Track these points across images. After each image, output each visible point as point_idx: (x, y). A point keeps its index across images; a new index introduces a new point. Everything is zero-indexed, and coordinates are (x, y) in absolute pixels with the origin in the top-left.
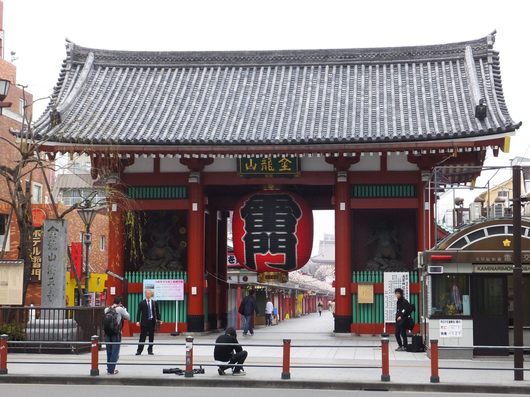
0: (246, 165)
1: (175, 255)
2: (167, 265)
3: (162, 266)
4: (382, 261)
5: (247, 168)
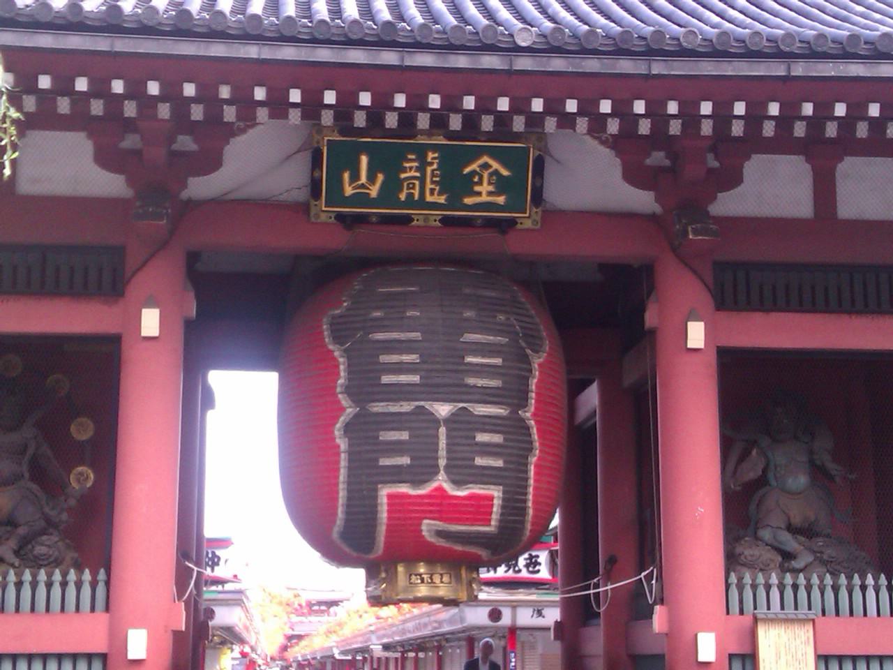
0: (346, 176)
1: (53, 513)
2: (21, 548)
4: (790, 542)
5: (349, 191)
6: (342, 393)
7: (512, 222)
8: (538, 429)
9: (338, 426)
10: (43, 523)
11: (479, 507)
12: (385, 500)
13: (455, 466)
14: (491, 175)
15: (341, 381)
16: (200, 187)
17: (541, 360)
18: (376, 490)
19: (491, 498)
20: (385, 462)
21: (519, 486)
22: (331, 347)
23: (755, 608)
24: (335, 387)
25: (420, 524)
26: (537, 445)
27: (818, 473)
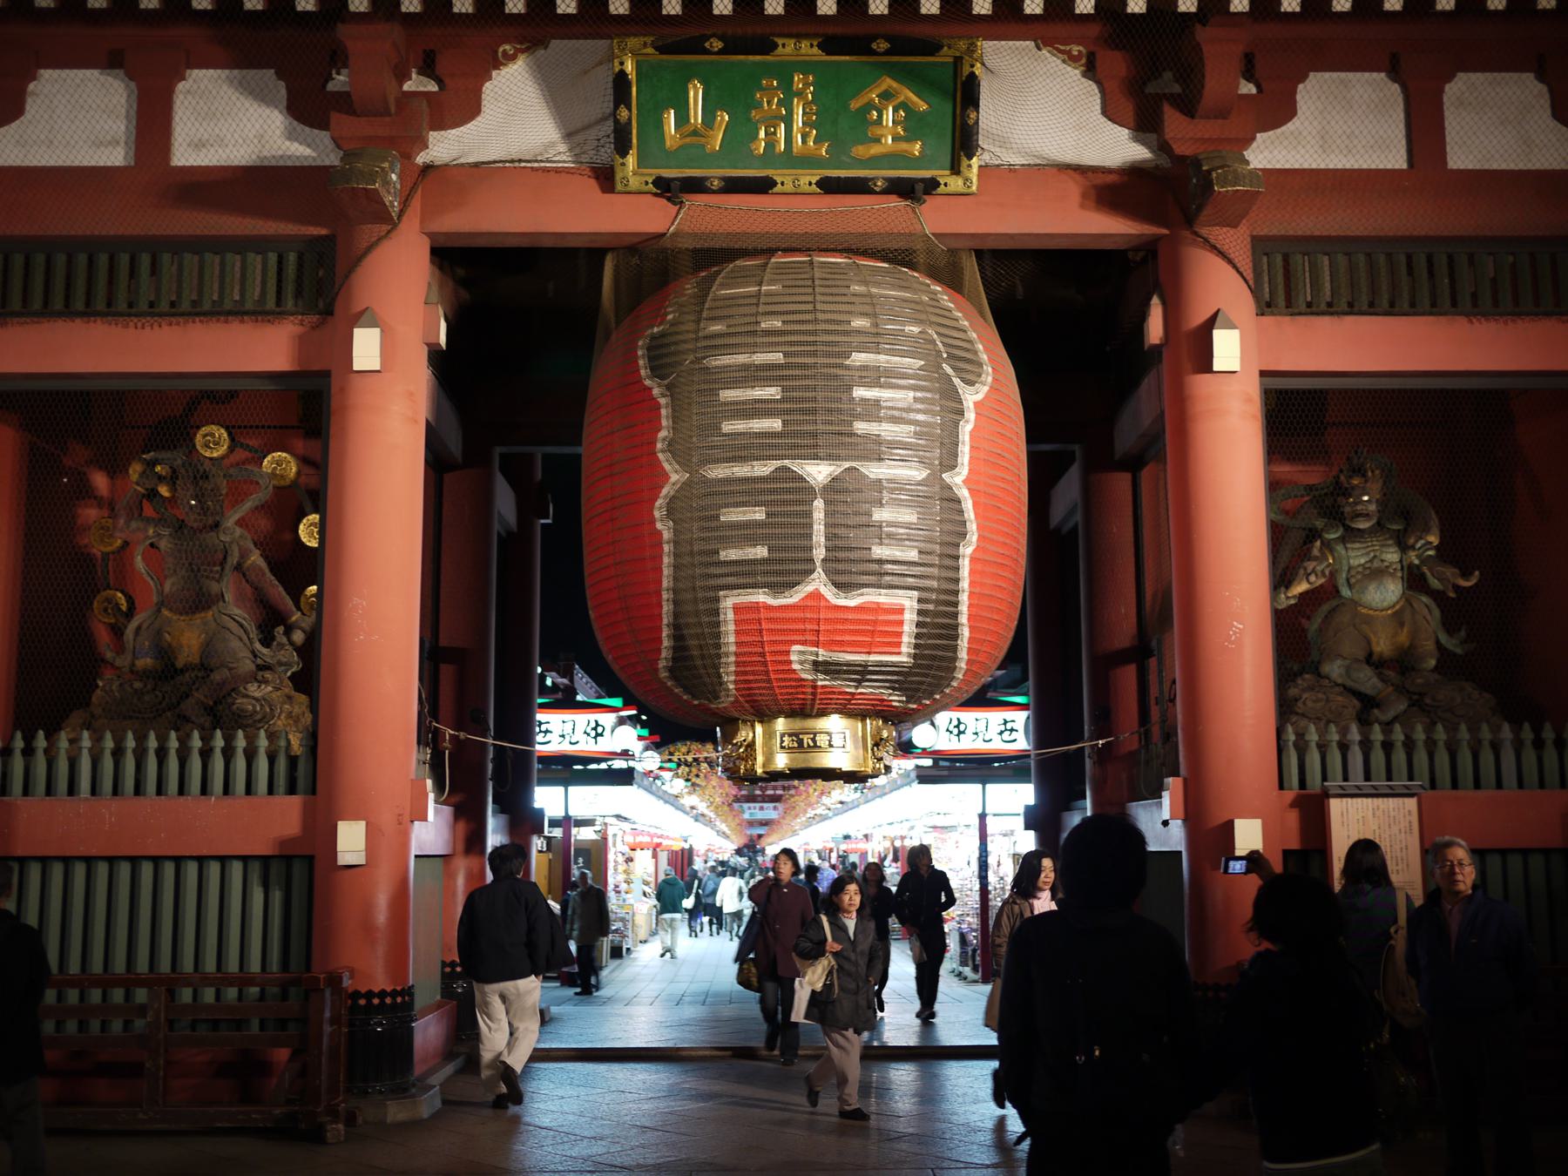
3: (188, 706)
6: (663, 451)
7: (931, 185)
8: (975, 504)
9: (659, 502)
10: (248, 665)
11: (879, 627)
12: (730, 615)
13: (838, 560)
14: (895, 110)
15: (663, 434)
16: (443, 147)
17: (980, 397)
18: (717, 600)
19: (901, 611)
20: (732, 554)
21: (947, 592)
22: (648, 382)
23: (1324, 779)
24: (654, 443)
25: (788, 652)
26: (972, 527)
27: (1414, 580)
